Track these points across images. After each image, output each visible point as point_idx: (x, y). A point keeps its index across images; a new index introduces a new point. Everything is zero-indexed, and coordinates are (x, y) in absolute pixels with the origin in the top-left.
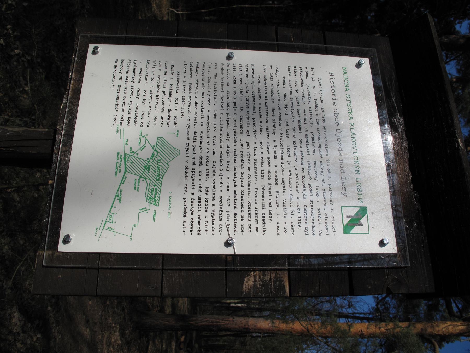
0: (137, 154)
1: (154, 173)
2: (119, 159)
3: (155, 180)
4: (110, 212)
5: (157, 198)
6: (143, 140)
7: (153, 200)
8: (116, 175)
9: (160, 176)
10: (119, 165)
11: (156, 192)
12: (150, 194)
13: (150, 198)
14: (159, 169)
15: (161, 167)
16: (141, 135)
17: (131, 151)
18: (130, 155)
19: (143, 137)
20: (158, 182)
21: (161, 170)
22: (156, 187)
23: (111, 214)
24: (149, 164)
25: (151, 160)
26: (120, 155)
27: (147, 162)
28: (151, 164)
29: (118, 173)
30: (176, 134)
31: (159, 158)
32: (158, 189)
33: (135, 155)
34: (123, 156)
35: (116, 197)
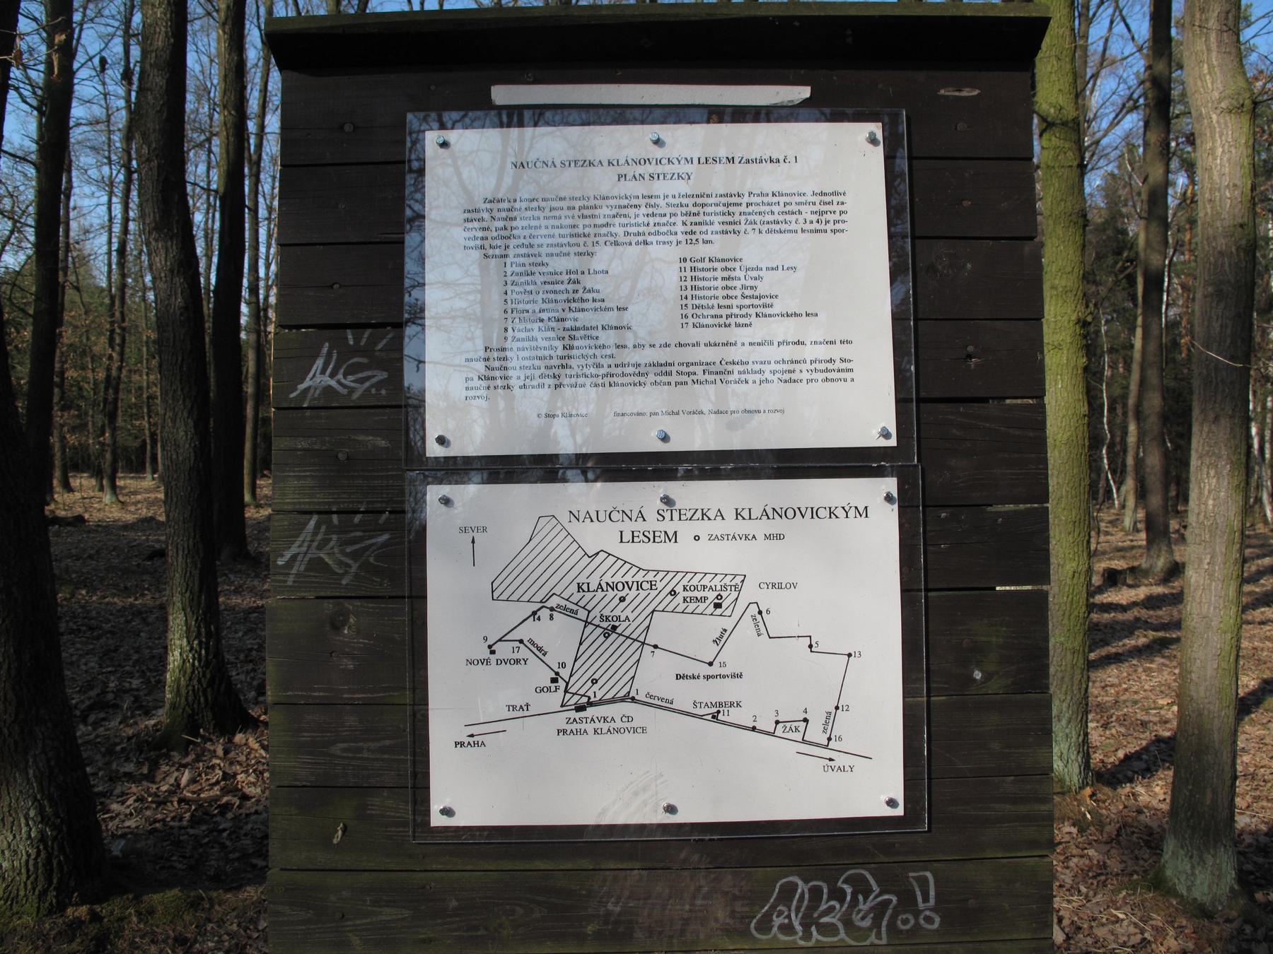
0: (563, 665)
1: (628, 600)
2: (583, 726)
3: (654, 593)
4: (772, 734)
5: (717, 581)
6: (504, 650)
7: (724, 594)
8: (644, 730)
9: (639, 577)
10: (605, 726)
11: (696, 588)
12: (702, 606)
14: (613, 587)
15: (607, 578)
16: (487, 662)
17: (549, 689)
18: (566, 691)
19: (493, 652)
20: (660, 586)
21: (616, 579)
22: (679, 589)
23: (779, 732)
24: (596, 622)
26: (569, 727)
27: (591, 628)
28: (595, 613)
29: (634, 724)
30: (475, 534)
31: (574, 587)
32: (685, 582)
33: (565, 673)
34: (573, 714)
35: (723, 723)
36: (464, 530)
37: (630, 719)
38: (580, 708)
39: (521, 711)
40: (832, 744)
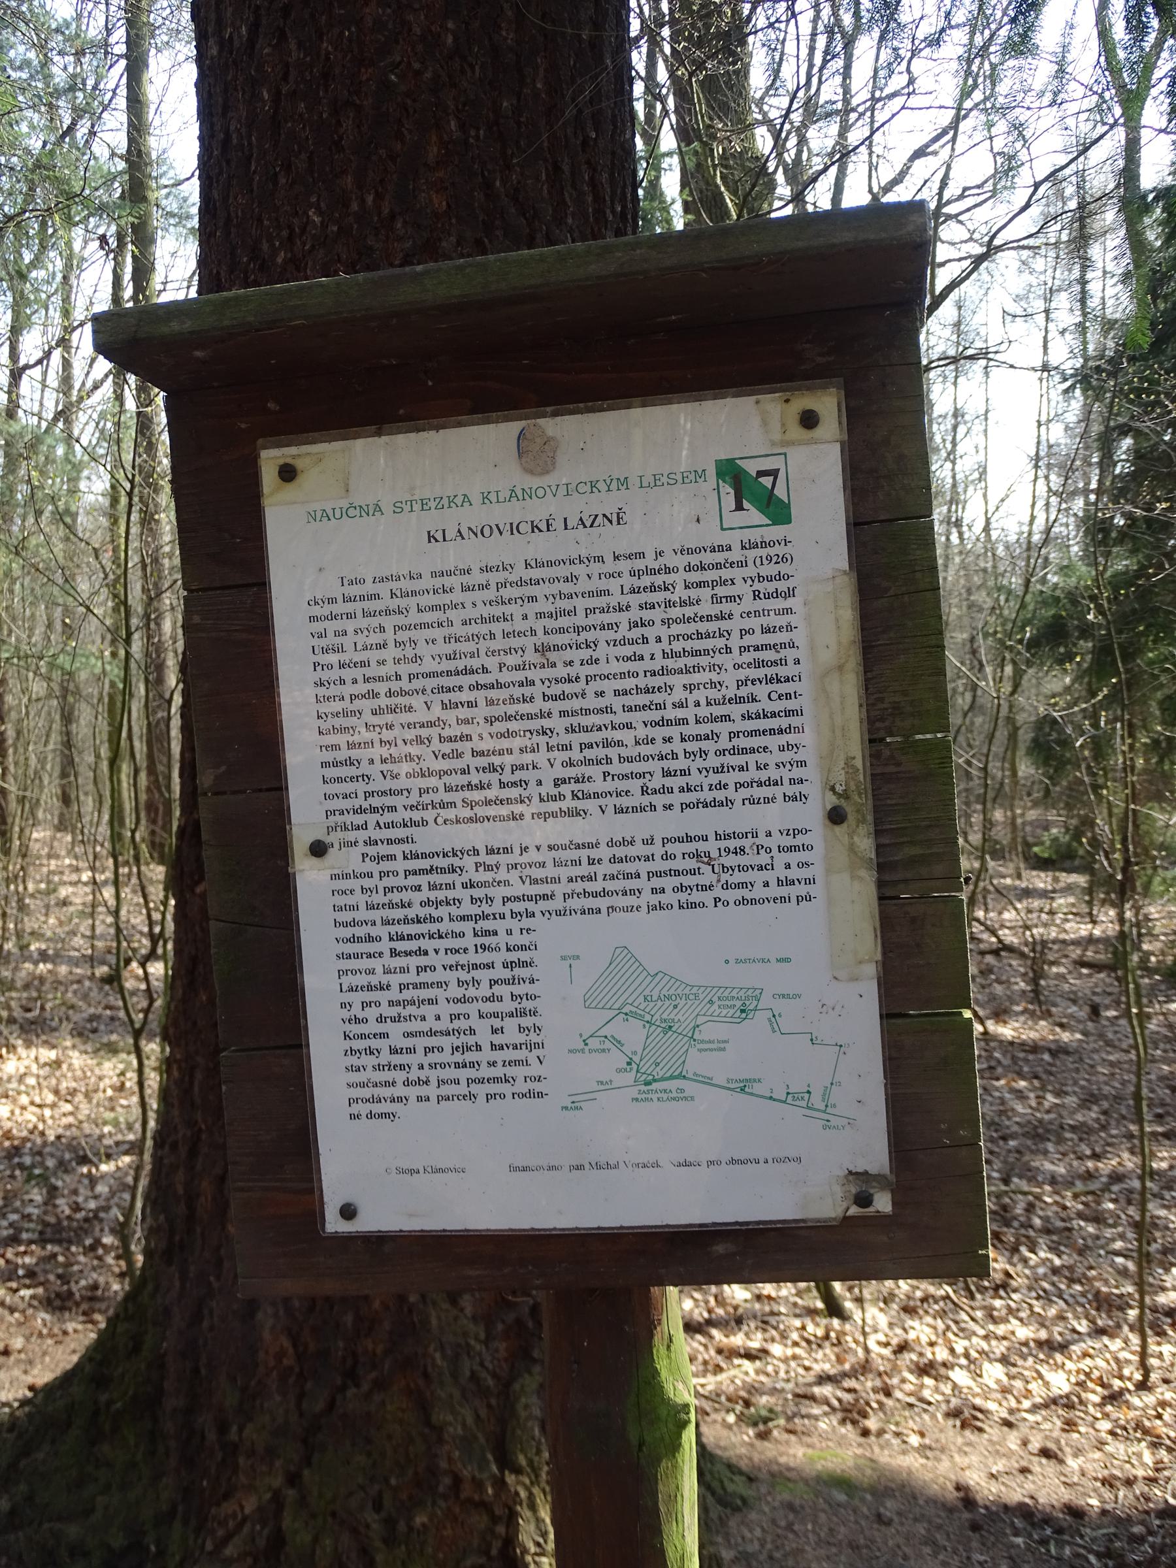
0: (635, 1053)
5: (742, 993)
6: (594, 1043)
8: (692, 1098)
9: (687, 991)
10: (665, 1096)
13: (743, 1011)
14: (669, 998)
15: (664, 992)
16: (583, 1051)
22: (715, 999)
23: (789, 1100)
25: (648, 1018)
28: (657, 1016)
31: (641, 998)
33: (636, 1059)
34: (643, 1088)
36: (563, 958)
37: (682, 1091)
38: (647, 1083)
39: (605, 1085)
40: (829, 1110)
